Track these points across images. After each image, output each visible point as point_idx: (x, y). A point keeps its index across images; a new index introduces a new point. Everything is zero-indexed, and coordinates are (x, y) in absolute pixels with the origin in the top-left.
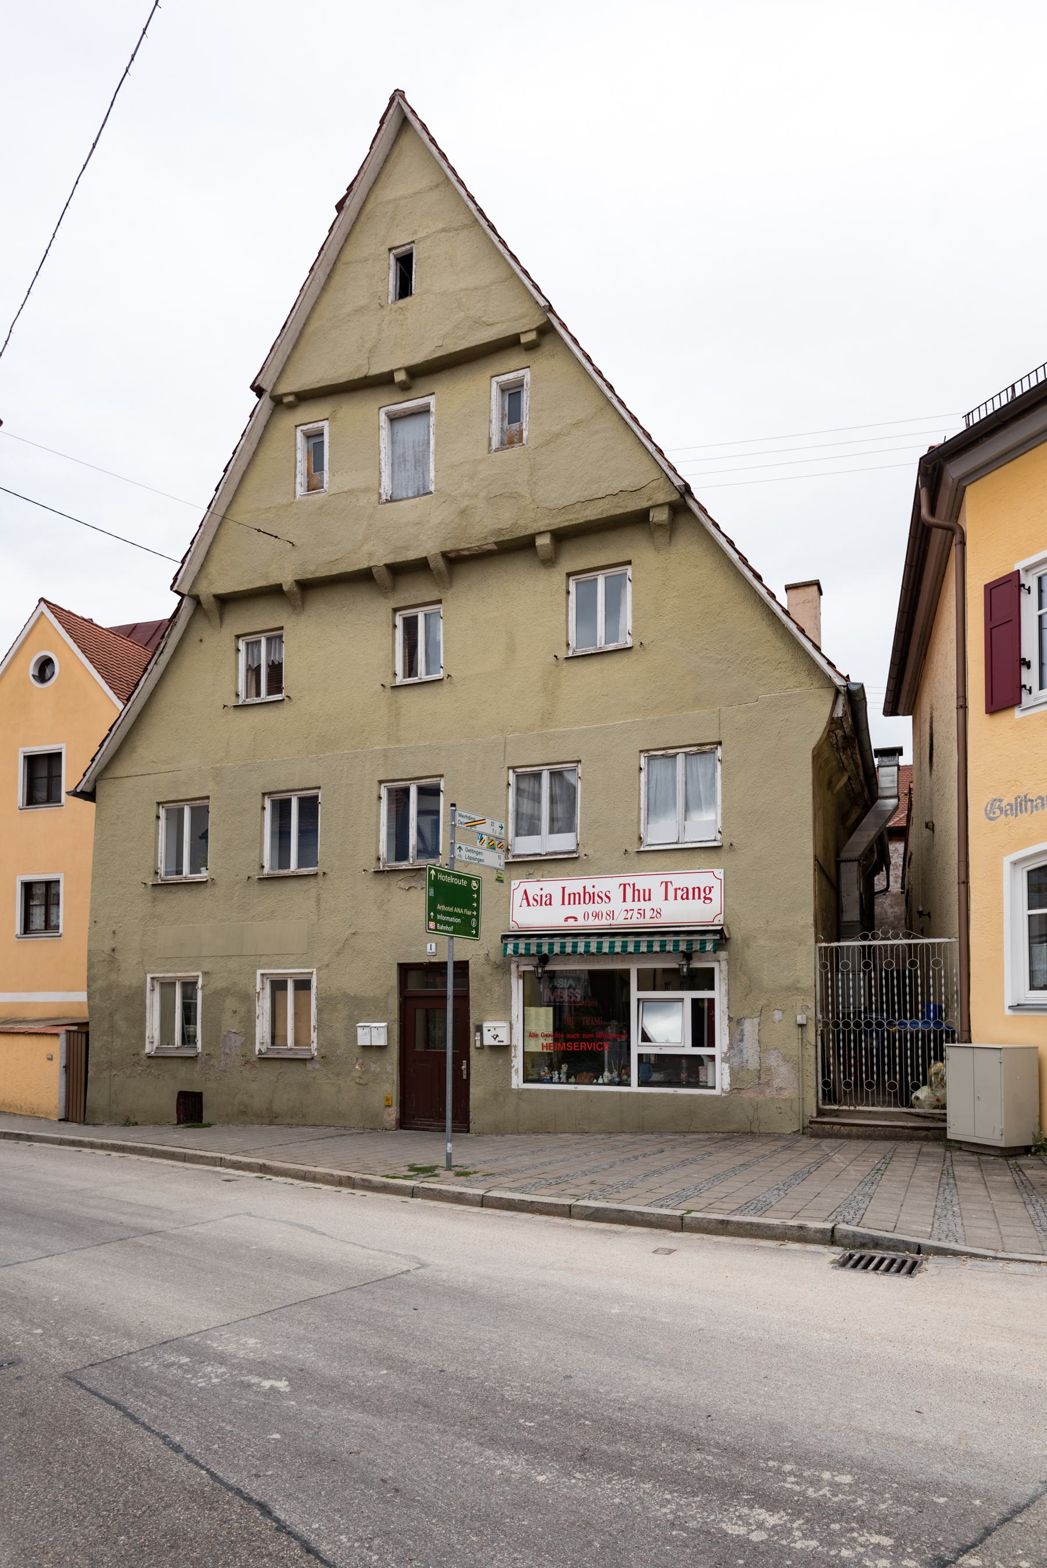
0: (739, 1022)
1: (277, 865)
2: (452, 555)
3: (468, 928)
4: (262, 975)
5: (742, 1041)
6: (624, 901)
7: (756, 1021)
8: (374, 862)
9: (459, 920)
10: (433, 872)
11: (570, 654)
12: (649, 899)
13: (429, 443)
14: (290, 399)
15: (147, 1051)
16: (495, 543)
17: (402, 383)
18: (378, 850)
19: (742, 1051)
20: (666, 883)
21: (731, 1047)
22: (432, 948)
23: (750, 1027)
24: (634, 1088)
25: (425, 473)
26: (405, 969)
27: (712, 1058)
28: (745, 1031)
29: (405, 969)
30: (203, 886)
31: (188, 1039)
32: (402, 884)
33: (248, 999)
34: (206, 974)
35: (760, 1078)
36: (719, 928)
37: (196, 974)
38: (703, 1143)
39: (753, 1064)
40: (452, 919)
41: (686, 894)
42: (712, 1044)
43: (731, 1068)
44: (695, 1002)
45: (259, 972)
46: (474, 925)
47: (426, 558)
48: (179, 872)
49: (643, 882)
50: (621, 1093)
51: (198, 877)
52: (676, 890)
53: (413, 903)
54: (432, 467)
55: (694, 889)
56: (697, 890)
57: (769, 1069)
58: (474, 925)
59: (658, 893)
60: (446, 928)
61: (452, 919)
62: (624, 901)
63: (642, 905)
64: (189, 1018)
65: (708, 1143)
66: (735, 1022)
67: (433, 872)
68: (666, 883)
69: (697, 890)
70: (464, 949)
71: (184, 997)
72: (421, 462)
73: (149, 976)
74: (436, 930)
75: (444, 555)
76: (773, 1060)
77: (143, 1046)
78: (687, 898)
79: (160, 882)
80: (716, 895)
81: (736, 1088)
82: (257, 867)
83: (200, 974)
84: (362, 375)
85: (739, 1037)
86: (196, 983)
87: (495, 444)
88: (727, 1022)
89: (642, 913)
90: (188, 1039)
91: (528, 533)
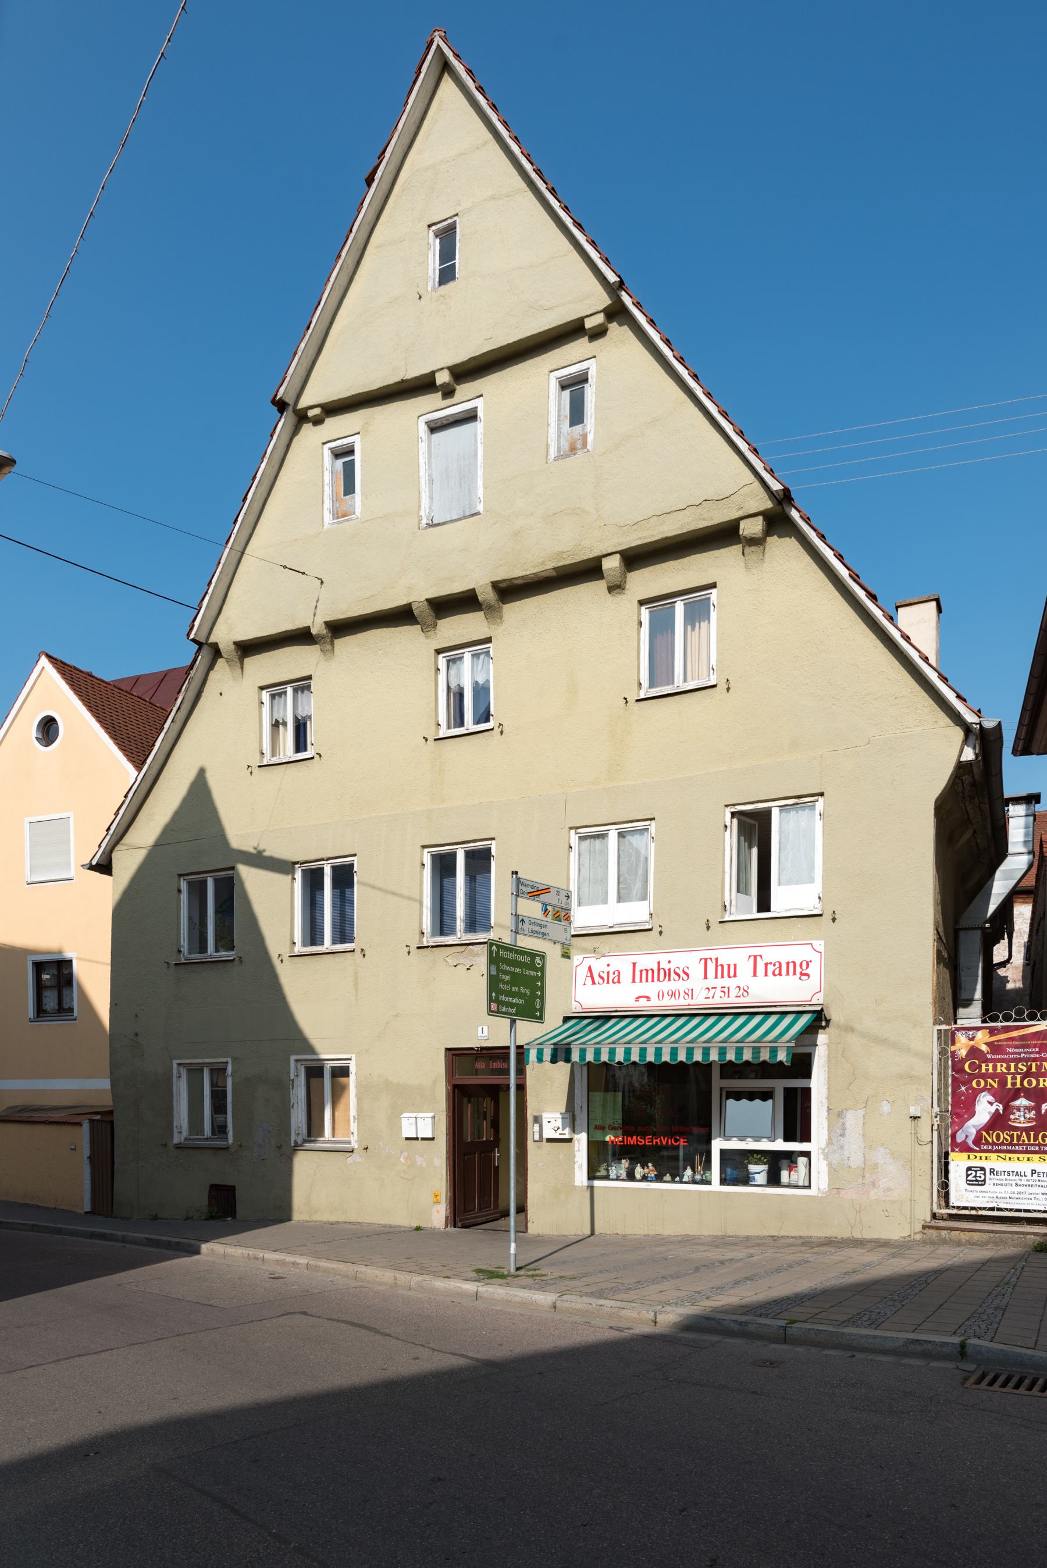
0: (840, 1114)
1: (309, 940)
2: (504, 585)
3: (533, 1011)
4: (297, 1061)
5: (843, 1135)
6: (706, 977)
7: (861, 1112)
8: (417, 936)
9: (522, 1001)
10: (494, 948)
11: (642, 696)
12: (735, 976)
13: (476, 455)
14: (317, 411)
15: (176, 1141)
16: (554, 569)
17: (444, 385)
18: (421, 923)
19: (842, 1147)
20: (755, 957)
21: (830, 1142)
22: (489, 1032)
23: (853, 1119)
24: (716, 1185)
25: (472, 490)
26: (457, 1057)
27: (807, 1154)
28: (847, 1126)
29: (457, 1057)
30: (230, 965)
31: (220, 1129)
32: (451, 961)
33: (283, 1086)
34: (234, 1059)
35: (864, 1177)
36: (819, 1008)
37: (225, 1060)
38: (798, 1248)
39: (856, 1161)
40: (514, 1000)
41: (778, 970)
42: (806, 1138)
43: (830, 1165)
44: (787, 1091)
45: (293, 1058)
46: (538, 1006)
47: (474, 589)
48: (203, 949)
49: (726, 957)
50: (700, 1192)
51: (224, 955)
52: (766, 965)
53: (468, 979)
54: (480, 483)
55: (788, 963)
56: (791, 965)
57: (875, 1166)
58: (538, 1006)
59: (745, 969)
60: (509, 1010)
61: (514, 1000)
62: (706, 977)
63: (726, 982)
64: (219, 1107)
65: (803, 1248)
66: (836, 1115)
67: (494, 948)
68: (755, 957)
69: (791, 965)
70: (527, 1032)
71: (213, 1085)
72: (466, 477)
73: (175, 1062)
74: (498, 1012)
75: (495, 585)
76: (880, 1156)
77: (172, 1138)
78: (780, 974)
79: (183, 961)
80: (814, 970)
81: (835, 1188)
82: (288, 943)
83: (229, 1060)
84: (398, 379)
85: (839, 1131)
86: (225, 1069)
87: (553, 452)
88: (825, 1114)
89: (726, 991)
90: (220, 1129)
91: (592, 556)
